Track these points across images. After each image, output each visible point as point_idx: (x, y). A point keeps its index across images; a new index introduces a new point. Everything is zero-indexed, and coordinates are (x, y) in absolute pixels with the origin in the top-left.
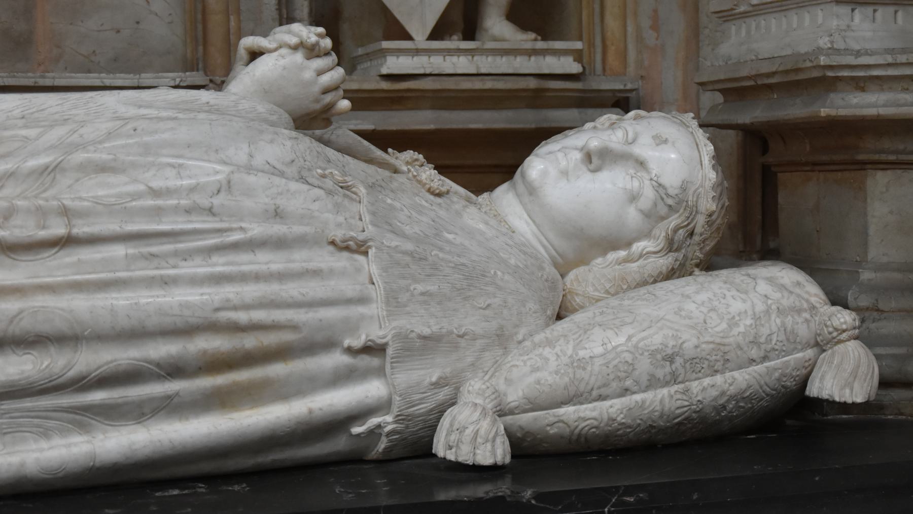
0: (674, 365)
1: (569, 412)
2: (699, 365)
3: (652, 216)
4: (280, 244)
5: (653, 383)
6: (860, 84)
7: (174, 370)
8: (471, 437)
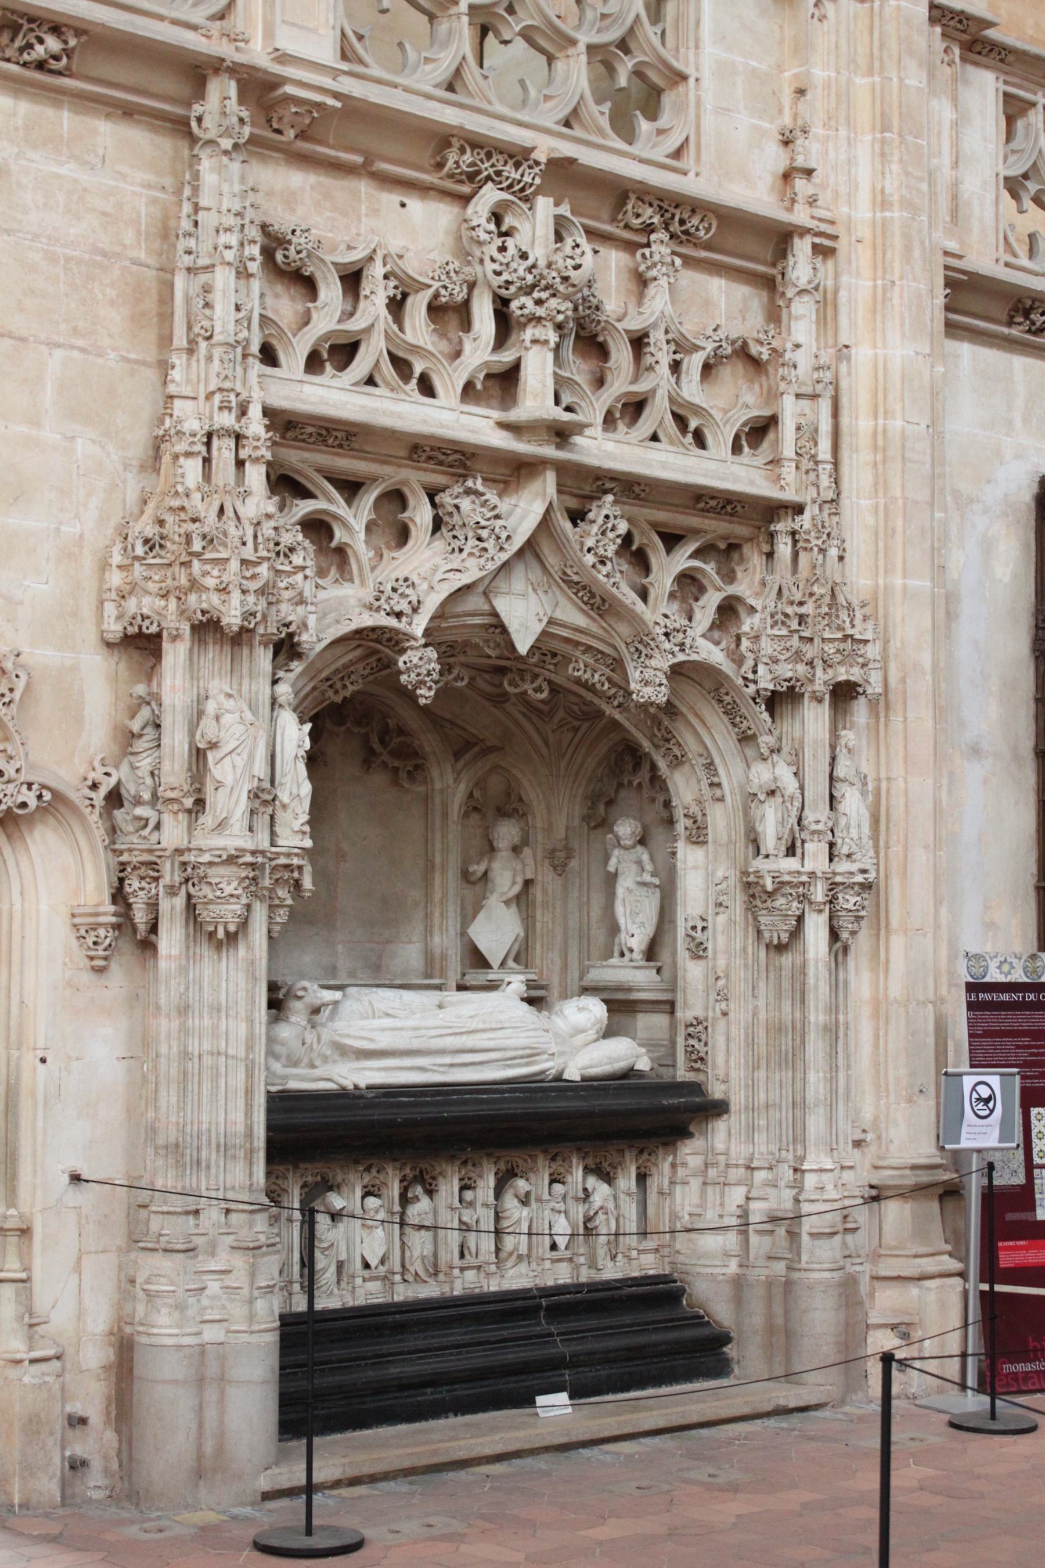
0: (611, 1060)
3: (594, 1025)
6: (639, 990)
7: (522, 1057)
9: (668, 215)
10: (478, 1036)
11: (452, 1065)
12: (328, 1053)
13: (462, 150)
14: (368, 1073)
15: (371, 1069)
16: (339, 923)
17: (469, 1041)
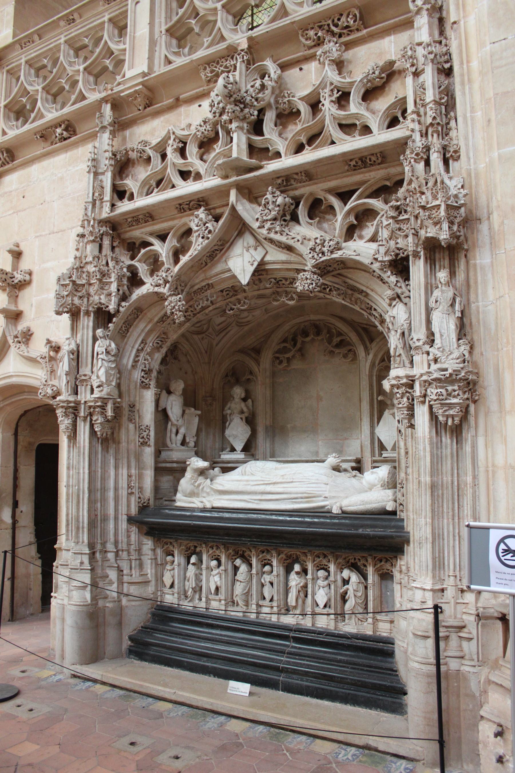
0: (364, 503)
1: (349, 508)
2: (367, 503)
4: (317, 483)
5: (360, 505)
7: (302, 498)
8: (335, 510)
9: (326, 27)
10: (279, 485)
11: (261, 500)
12: (208, 491)
13: (205, 69)
14: (223, 501)
15: (224, 499)
16: (319, 431)
17: (269, 488)
